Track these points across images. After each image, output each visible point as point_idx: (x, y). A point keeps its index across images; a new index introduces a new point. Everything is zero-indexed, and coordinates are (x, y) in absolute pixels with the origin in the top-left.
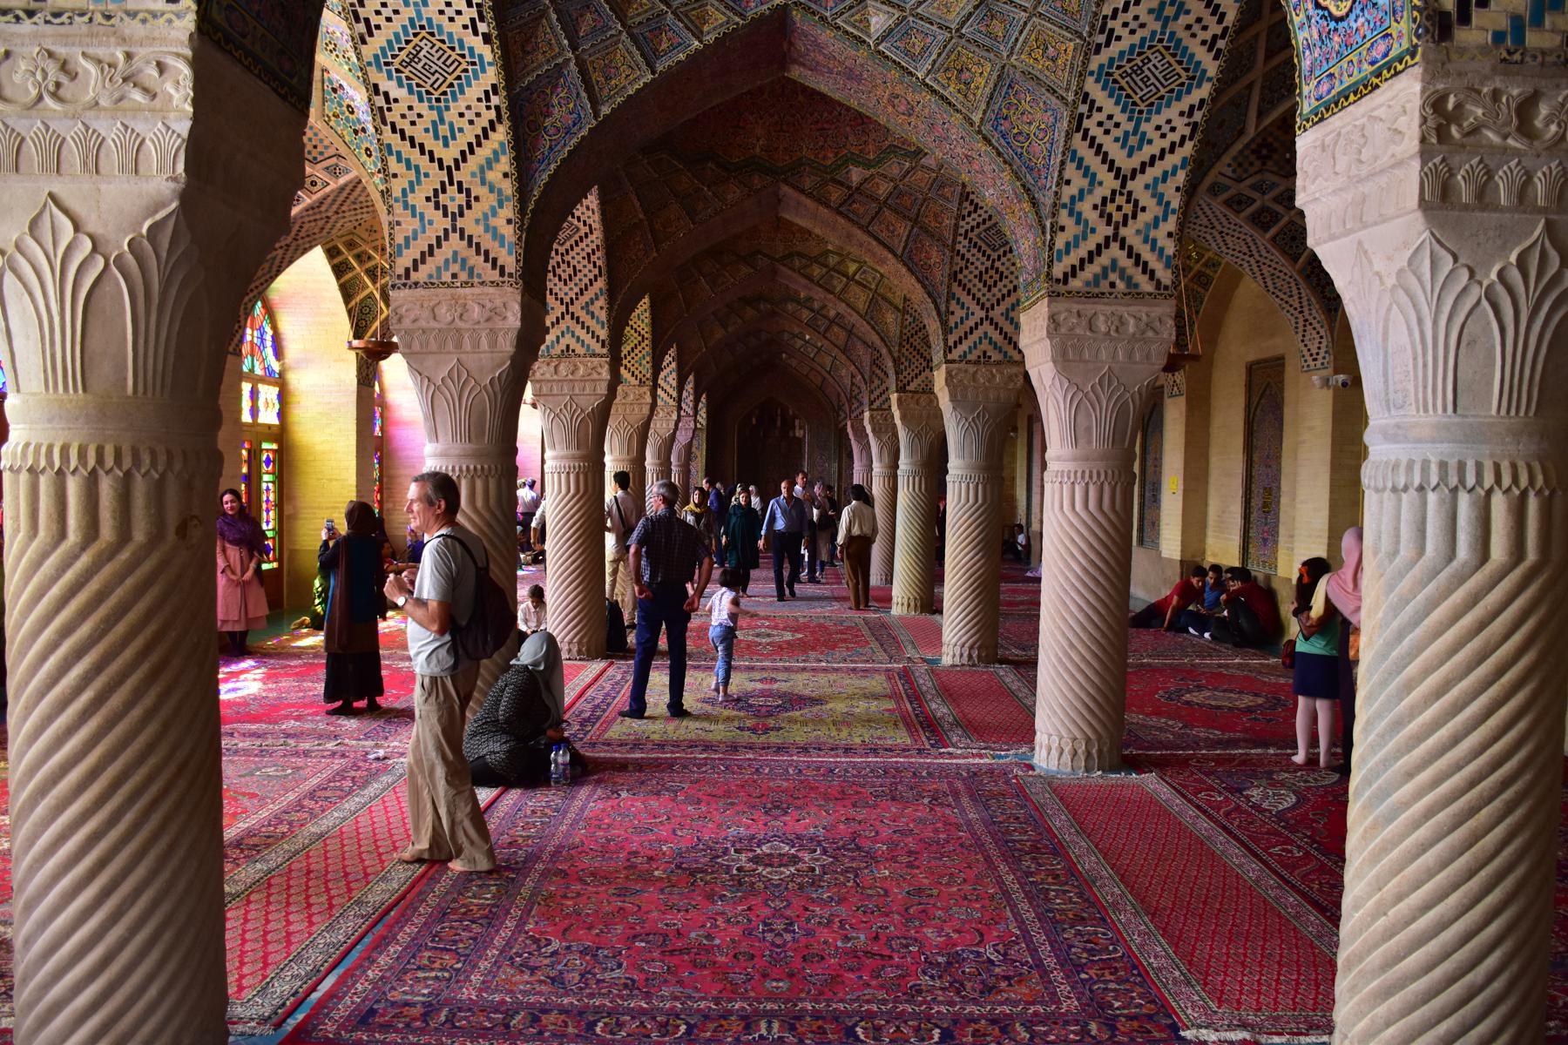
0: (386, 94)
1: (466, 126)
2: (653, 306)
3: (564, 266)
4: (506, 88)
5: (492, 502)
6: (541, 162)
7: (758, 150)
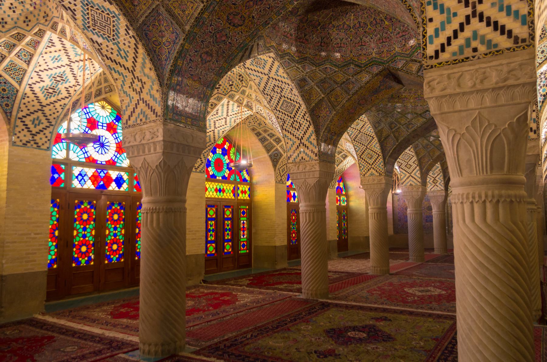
0: (97, 42)
1: (129, 49)
2: (379, 141)
3: (295, 123)
4: (131, 25)
5: (161, 224)
6: (166, 60)
7: (374, 55)
